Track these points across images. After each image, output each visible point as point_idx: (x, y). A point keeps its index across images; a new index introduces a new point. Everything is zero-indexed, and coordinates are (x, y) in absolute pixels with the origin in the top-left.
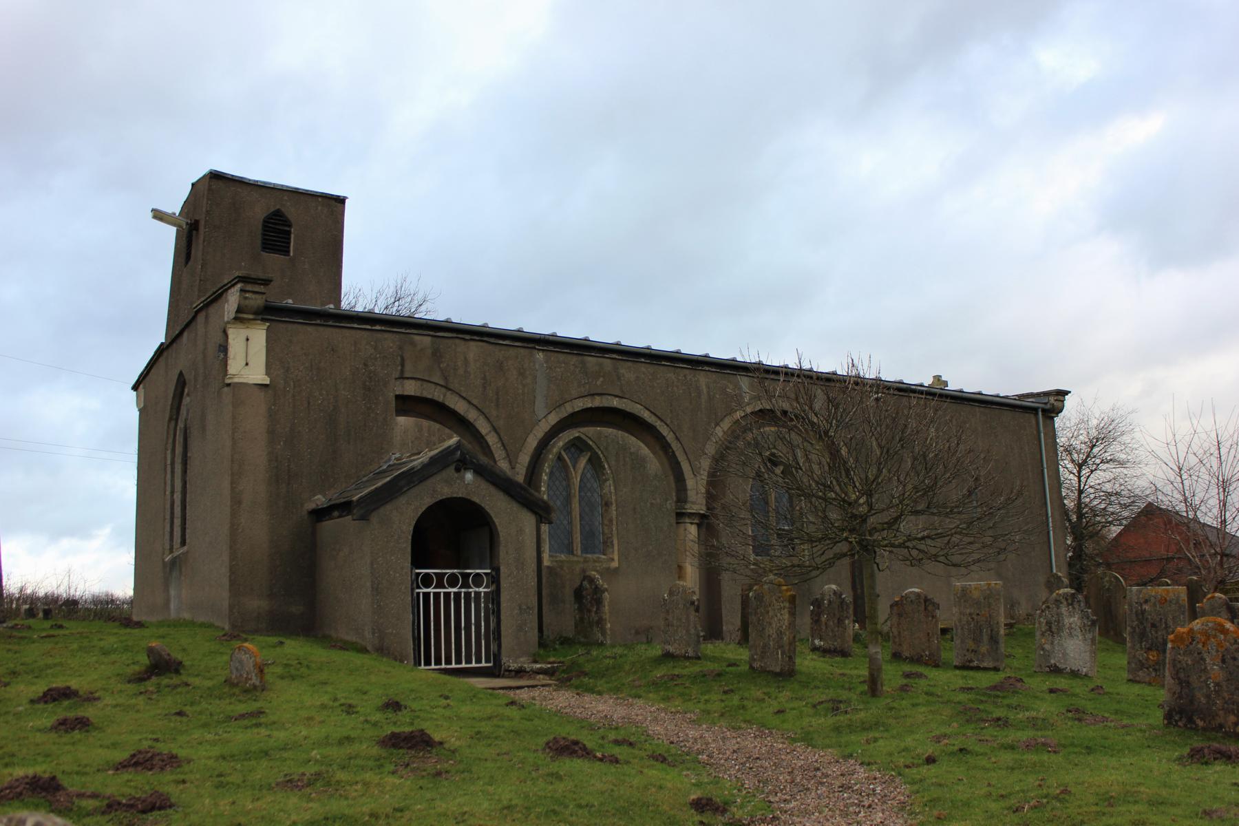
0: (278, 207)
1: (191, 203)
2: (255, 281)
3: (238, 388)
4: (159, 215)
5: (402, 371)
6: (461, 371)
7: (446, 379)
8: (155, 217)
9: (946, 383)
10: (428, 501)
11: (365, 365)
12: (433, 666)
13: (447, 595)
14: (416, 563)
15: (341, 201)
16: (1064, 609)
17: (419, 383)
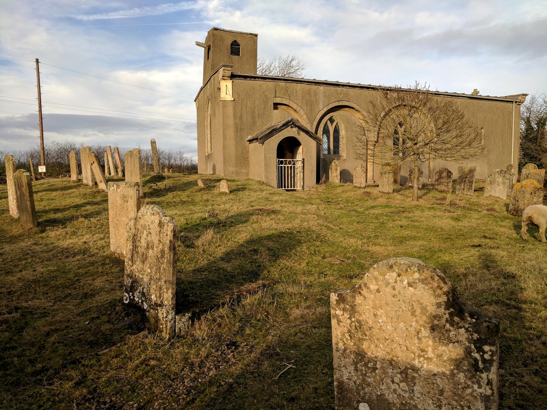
1: (208, 39)
3: (224, 102)
4: (198, 44)
6: (295, 94)
8: (197, 45)
9: (479, 92)
10: (282, 138)
11: (264, 93)
12: (283, 188)
13: (288, 167)
14: (279, 156)
15: (256, 35)
16: (497, 175)
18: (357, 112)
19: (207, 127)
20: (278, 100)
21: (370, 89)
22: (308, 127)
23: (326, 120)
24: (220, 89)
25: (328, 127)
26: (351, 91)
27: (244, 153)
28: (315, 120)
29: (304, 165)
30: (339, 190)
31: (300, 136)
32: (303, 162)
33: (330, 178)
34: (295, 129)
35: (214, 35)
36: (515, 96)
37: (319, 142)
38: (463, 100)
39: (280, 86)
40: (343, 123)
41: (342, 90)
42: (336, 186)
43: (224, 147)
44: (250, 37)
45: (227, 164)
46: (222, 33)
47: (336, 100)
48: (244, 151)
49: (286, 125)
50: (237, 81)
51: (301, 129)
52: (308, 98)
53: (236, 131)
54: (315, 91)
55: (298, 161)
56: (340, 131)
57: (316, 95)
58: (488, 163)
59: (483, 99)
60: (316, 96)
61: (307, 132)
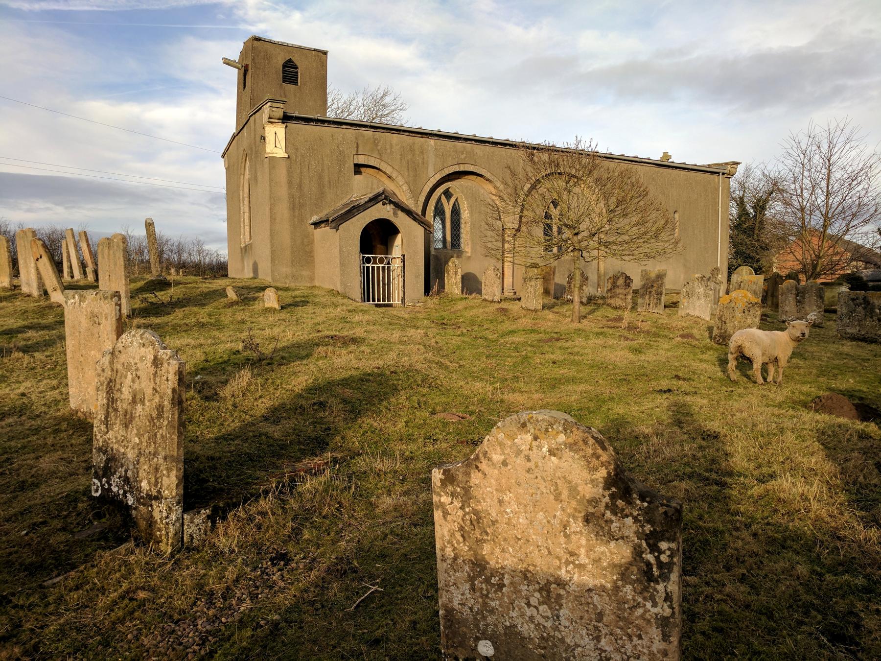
1: (243, 54)
2: (277, 101)
3: (272, 159)
4: (227, 62)
5: (357, 151)
6: (389, 151)
11: (338, 147)
12: (371, 302)
13: (378, 268)
16: (696, 284)
18: (488, 182)
19: (243, 200)
20: (361, 160)
21: (508, 147)
22: (410, 204)
23: (439, 194)
25: (442, 205)
26: (479, 149)
29: (404, 265)
30: (460, 305)
31: (398, 219)
32: (403, 261)
33: (446, 287)
34: (389, 207)
35: (253, 49)
36: (722, 164)
37: (428, 229)
38: (648, 168)
40: (467, 199)
41: (464, 147)
42: (456, 300)
43: (272, 234)
45: (277, 262)
47: (454, 162)
48: (305, 240)
49: (374, 200)
50: (293, 126)
52: (409, 157)
53: (293, 209)
54: (421, 147)
56: (462, 211)
57: (422, 153)
58: (685, 266)
59: (676, 168)
60: (423, 154)
61: (409, 212)
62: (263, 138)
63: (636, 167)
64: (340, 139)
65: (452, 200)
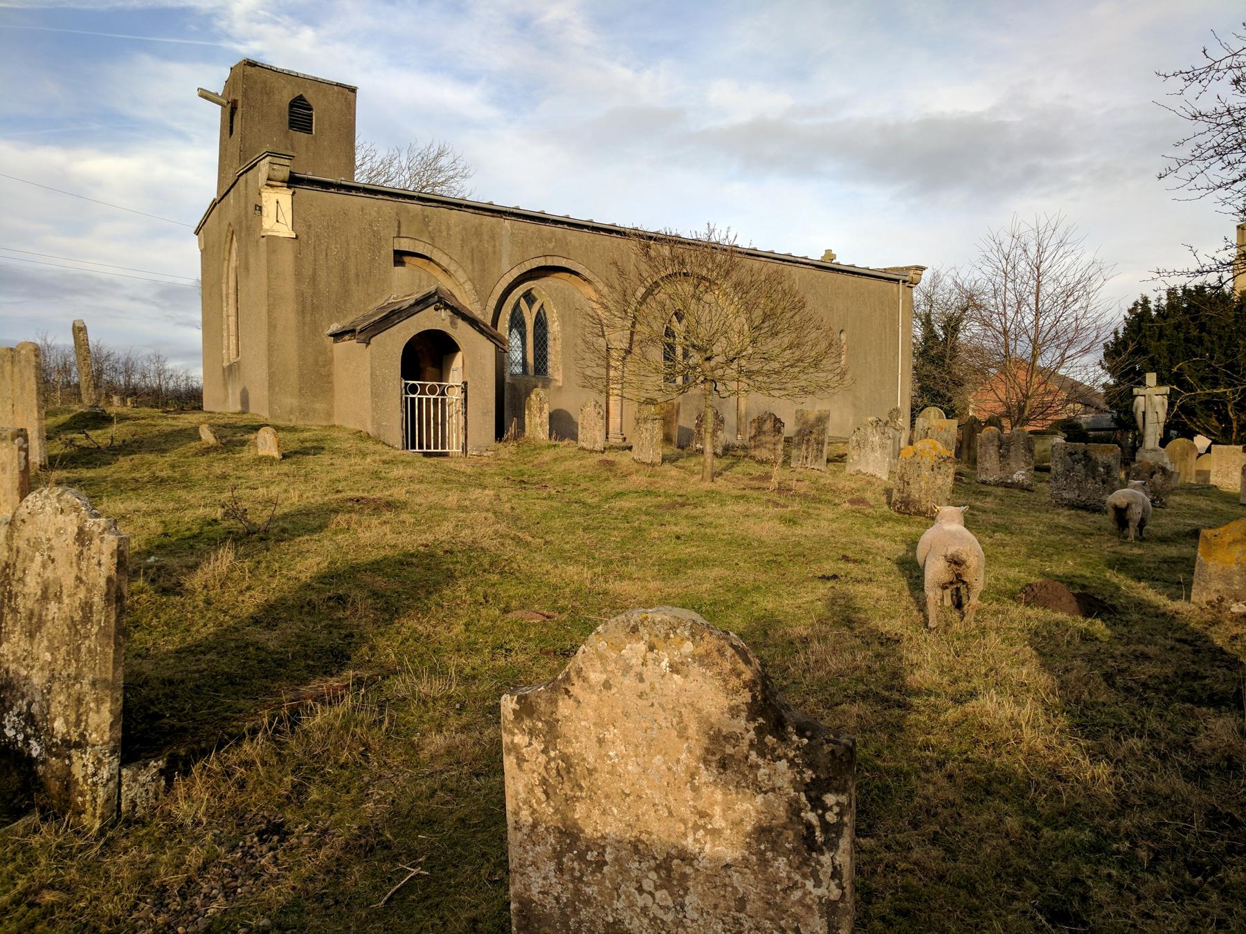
0: (301, 93)
1: (230, 84)
2: (279, 155)
3: (272, 240)
4: (205, 95)
5: (399, 232)
6: (445, 233)
7: (433, 239)
8: (201, 96)
10: (414, 332)
12: (417, 450)
14: (405, 375)
16: (869, 430)
17: (412, 241)
20: (405, 245)
22: (475, 310)
23: (517, 298)
24: (260, 209)
25: (521, 312)
26: (573, 236)
27: (321, 363)
28: (492, 296)
29: (466, 396)
30: (547, 456)
31: (458, 330)
32: (465, 391)
33: (527, 429)
34: (445, 314)
35: (245, 77)
36: (902, 268)
37: (501, 346)
38: (805, 271)
39: (408, 212)
40: (556, 305)
41: (553, 233)
42: (541, 448)
43: (271, 348)
44: (338, 93)
45: (277, 389)
46: (268, 74)
47: (539, 253)
48: (321, 359)
49: (423, 303)
50: (305, 192)
51: (459, 313)
52: (474, 243)
53: (302, 312)
55: (452, 386)
56: (549, 323)
57: (493, 238)
58: (854, 405)
59: (843, 271)
61: (473, 322)
62: (259, 208)
63: (789, 268)
64: (375, 214)
65: (536, 307)
